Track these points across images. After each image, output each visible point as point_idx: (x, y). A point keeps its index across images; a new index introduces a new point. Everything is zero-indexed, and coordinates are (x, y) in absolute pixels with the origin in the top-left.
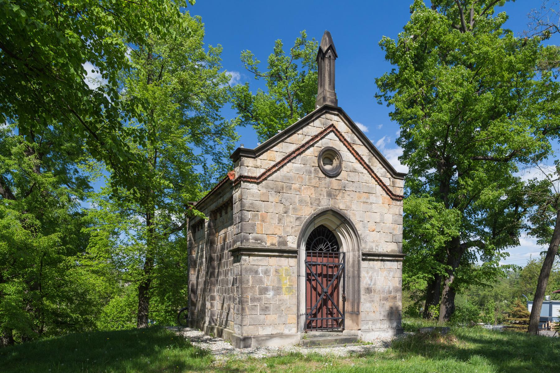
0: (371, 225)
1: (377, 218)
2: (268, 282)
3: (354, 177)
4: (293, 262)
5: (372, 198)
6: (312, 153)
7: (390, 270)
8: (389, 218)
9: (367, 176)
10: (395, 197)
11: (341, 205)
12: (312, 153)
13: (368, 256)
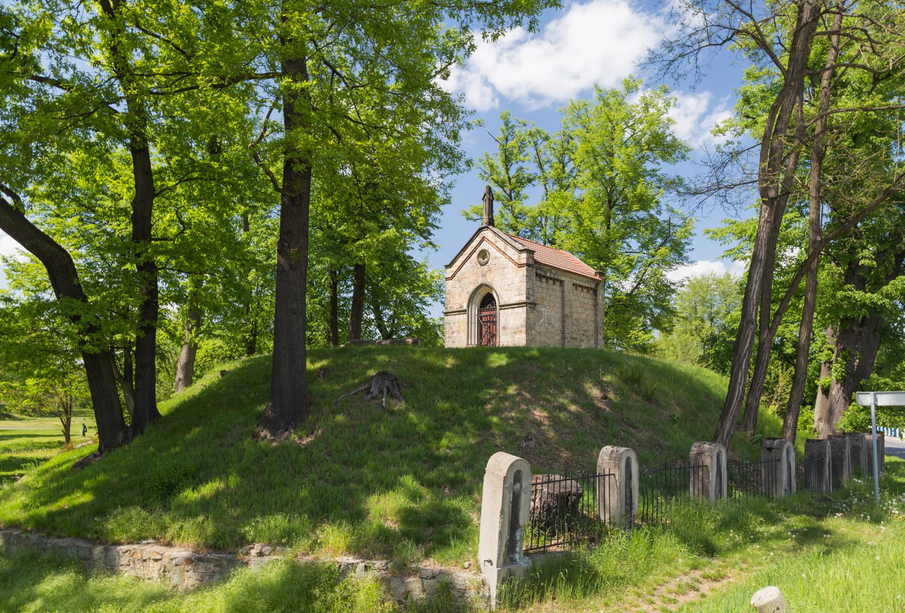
0: (506, 287)
1: (509, 282)
2: (455, 329)
3: (495, 261)
4: (465, 316)
5: (506, 270)
6: (475, 255)
7: (518, 313)
8: (517, 280)
9: (503, 258)
10: (520, 266)
11: (488, 280)
12: (475, 255)
13: (503, 307)
